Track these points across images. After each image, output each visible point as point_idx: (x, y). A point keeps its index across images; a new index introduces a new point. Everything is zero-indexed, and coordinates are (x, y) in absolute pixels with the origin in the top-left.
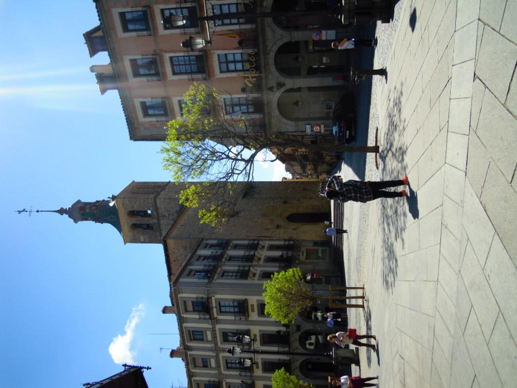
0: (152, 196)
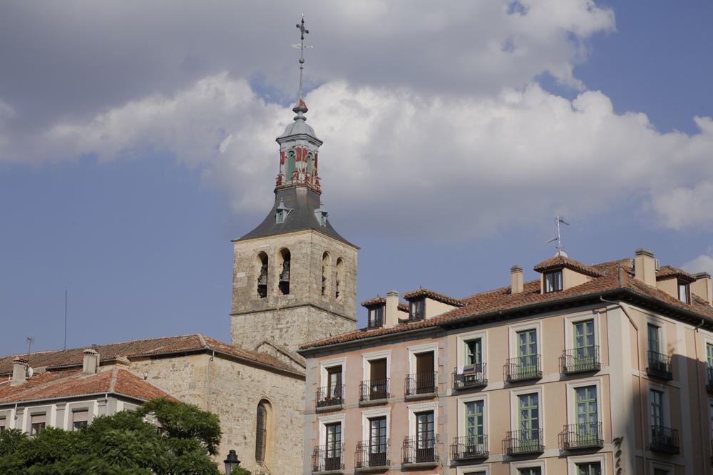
0: (316, 298)
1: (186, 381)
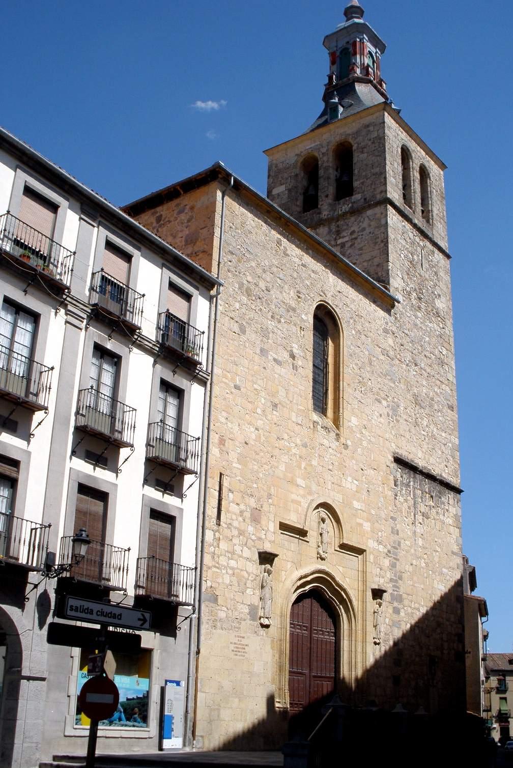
1: (180, 235)
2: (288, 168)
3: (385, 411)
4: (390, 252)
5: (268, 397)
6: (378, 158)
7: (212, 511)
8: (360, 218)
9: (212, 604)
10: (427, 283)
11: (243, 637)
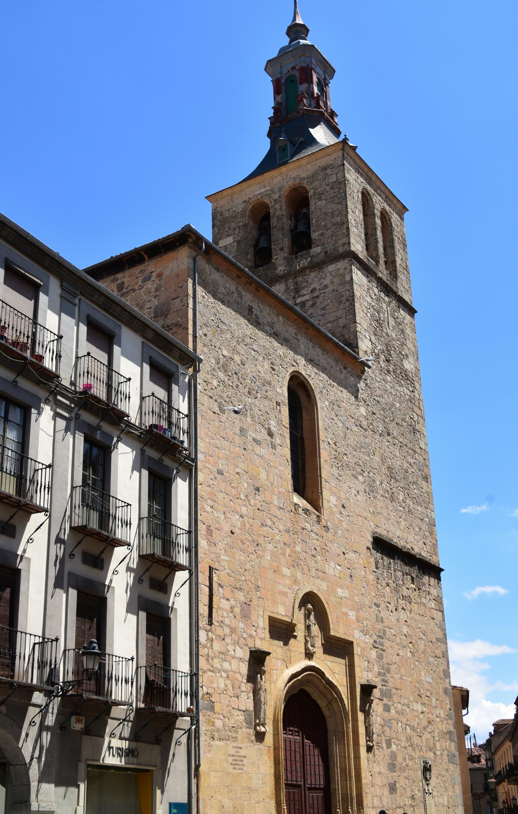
1: (148, 305)
2: (236, 217)
3: (361, 488)
4: (357, 311)
5: (250, 481)
6: (339, 205)
7: (203, 610)
8: (320, 274)
9: (209, 713)
10: (394, 343)
11: (241, 748)
